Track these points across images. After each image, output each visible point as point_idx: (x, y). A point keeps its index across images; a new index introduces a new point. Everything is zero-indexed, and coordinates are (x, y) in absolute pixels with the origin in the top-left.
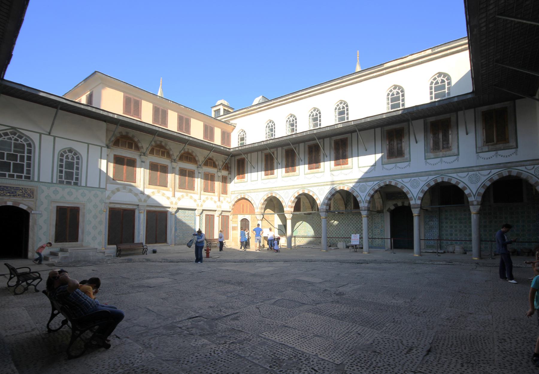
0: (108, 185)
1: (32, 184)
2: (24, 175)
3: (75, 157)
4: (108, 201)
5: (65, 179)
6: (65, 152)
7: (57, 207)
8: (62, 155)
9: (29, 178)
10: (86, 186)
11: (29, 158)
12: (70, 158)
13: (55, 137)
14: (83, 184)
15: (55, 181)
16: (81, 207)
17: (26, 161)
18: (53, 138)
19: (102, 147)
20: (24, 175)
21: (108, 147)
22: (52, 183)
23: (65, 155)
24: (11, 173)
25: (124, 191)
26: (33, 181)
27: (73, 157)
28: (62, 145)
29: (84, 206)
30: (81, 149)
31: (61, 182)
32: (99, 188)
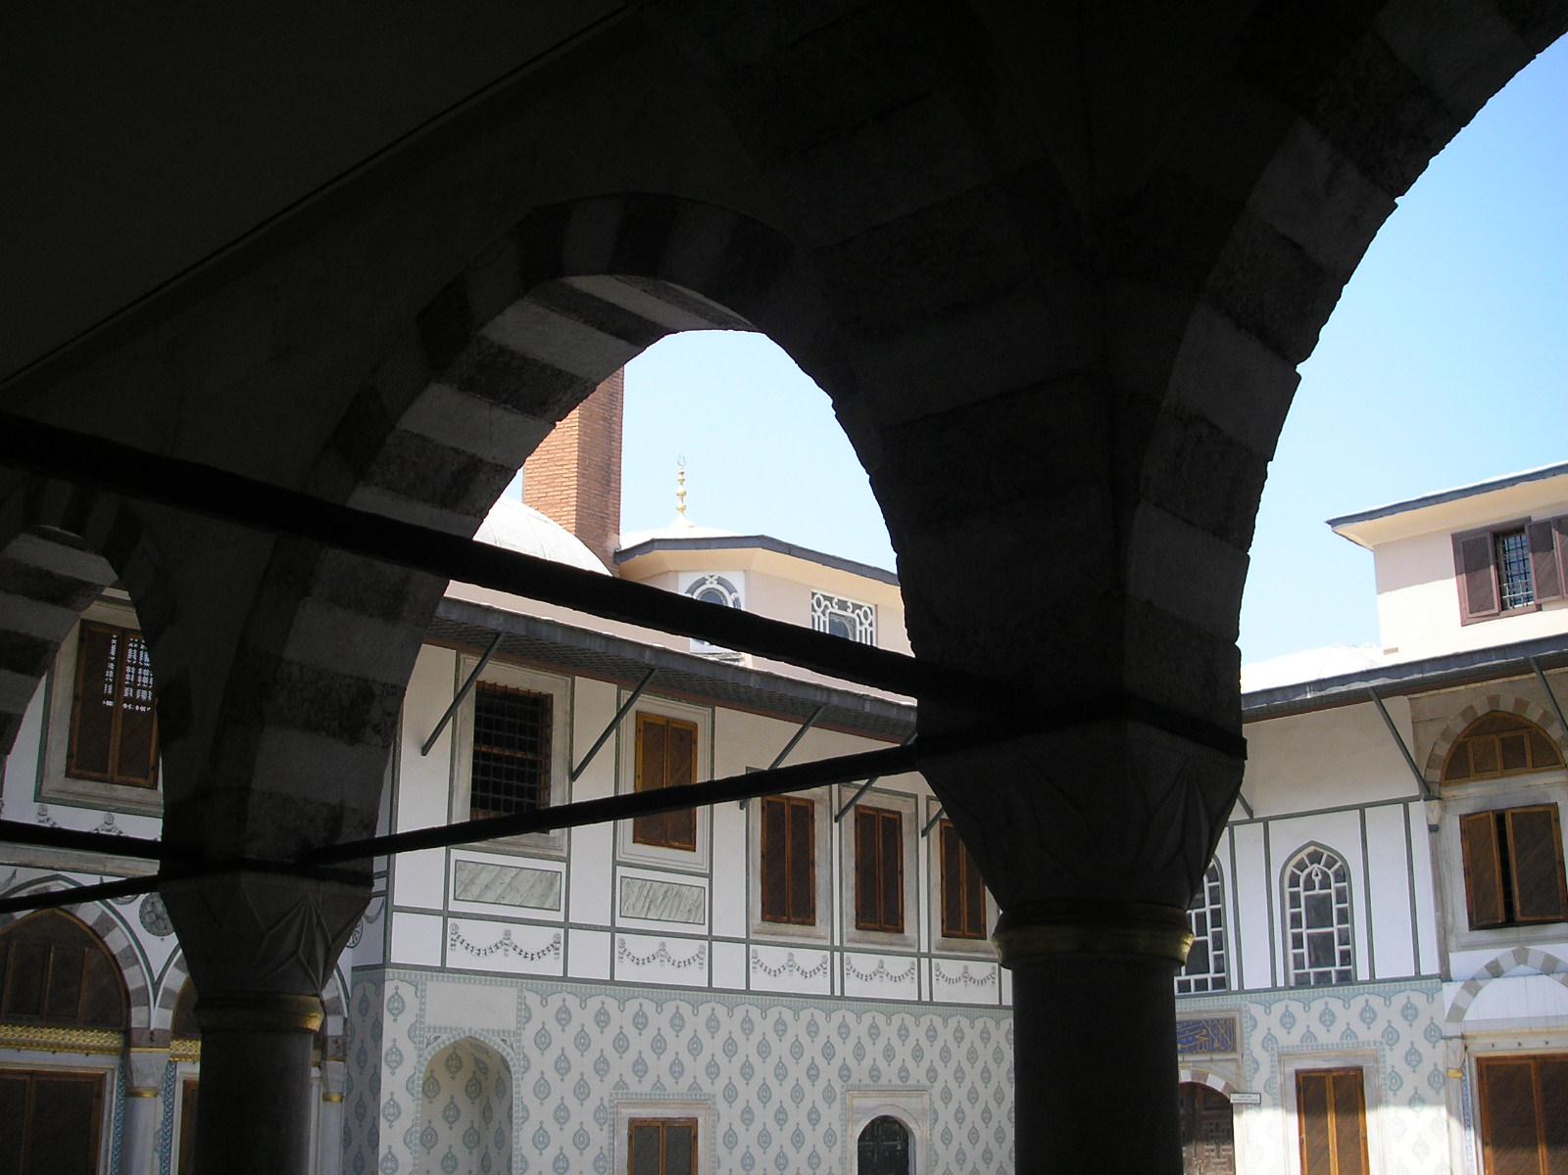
0: (1452, 956)
1: (1228, 1002)
2: (1210, 976)
3: (1329, 872)
4: (1452, 1029)
5: (1310, 967)
6: (1301, 866)
7: (1298, 1073)
8: (1294, 881)
9: (1220, 983)
10: (1373, 980)
11: (1218, 917)
12: (1317, 880)
13: (1266, 821)
14: (1363, 974)
15: (1281, 983)
16: (1367, 1066)
17: (1210, 930)
18: (1261, 825)
19: (1405, 802)
20: (1210, 976)
21: (1429, 792)
22: (1274, 988)
23: (1303, 876)
24: (1183, 977)
25: (1522, 968)
26: (1231, 993)
27: (1325, 875)
28: (1288, 840)
29: (1376, 1061)
30: (1340, 836)
31: (1302, 982)
32: (1418, 976)
